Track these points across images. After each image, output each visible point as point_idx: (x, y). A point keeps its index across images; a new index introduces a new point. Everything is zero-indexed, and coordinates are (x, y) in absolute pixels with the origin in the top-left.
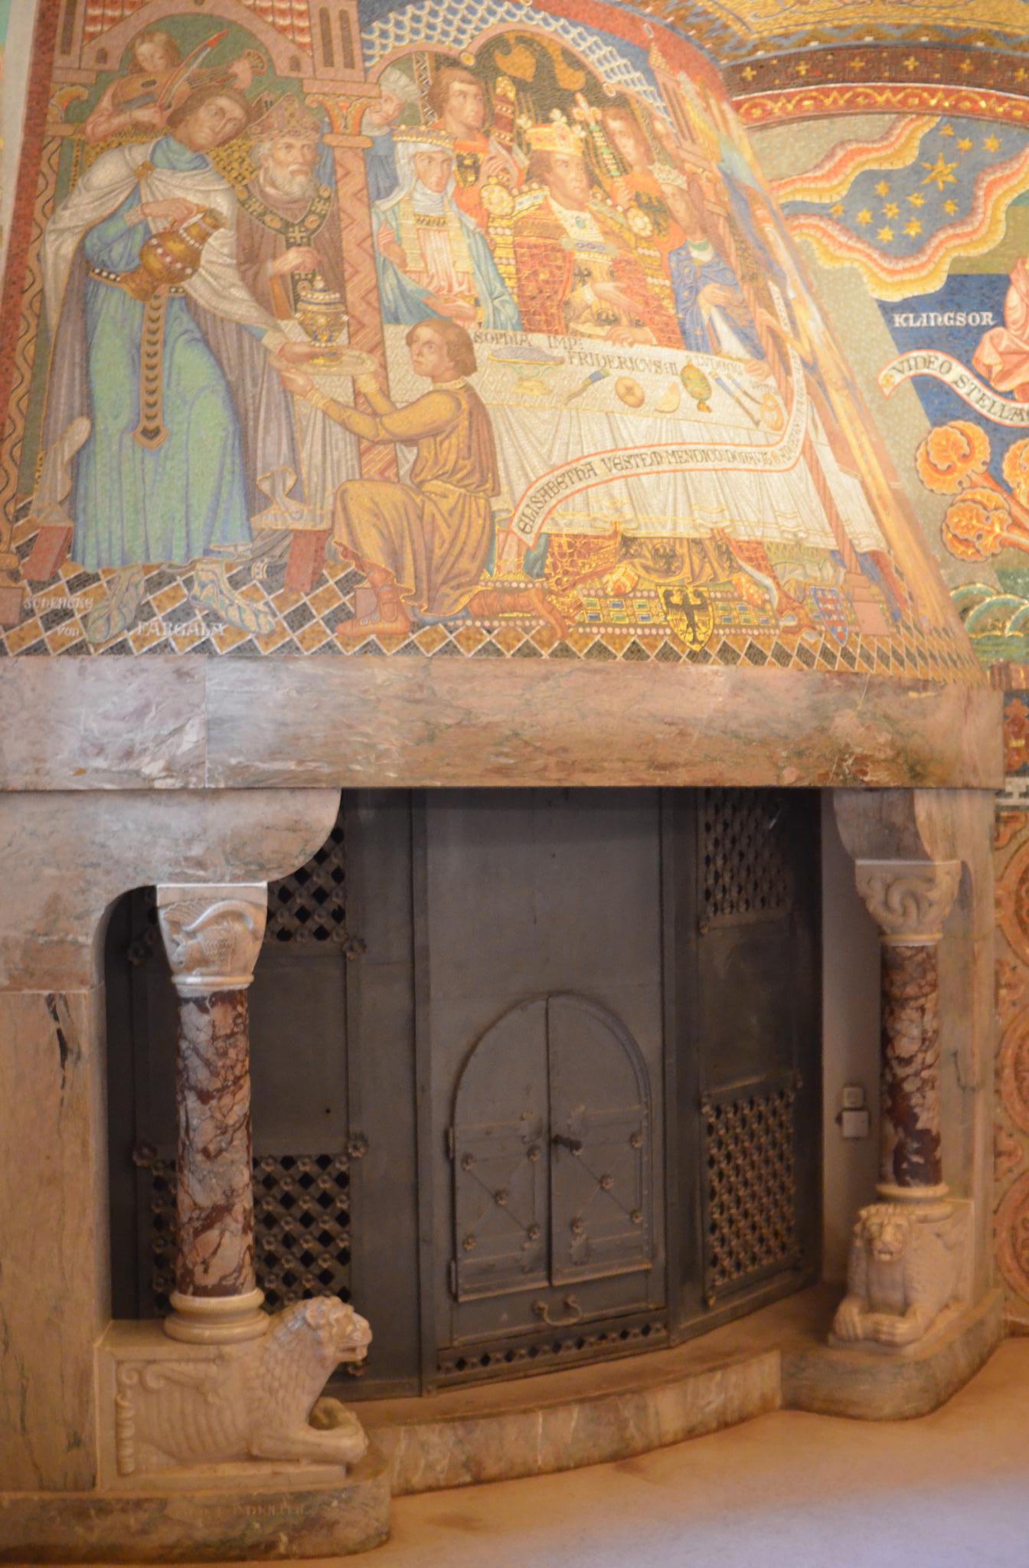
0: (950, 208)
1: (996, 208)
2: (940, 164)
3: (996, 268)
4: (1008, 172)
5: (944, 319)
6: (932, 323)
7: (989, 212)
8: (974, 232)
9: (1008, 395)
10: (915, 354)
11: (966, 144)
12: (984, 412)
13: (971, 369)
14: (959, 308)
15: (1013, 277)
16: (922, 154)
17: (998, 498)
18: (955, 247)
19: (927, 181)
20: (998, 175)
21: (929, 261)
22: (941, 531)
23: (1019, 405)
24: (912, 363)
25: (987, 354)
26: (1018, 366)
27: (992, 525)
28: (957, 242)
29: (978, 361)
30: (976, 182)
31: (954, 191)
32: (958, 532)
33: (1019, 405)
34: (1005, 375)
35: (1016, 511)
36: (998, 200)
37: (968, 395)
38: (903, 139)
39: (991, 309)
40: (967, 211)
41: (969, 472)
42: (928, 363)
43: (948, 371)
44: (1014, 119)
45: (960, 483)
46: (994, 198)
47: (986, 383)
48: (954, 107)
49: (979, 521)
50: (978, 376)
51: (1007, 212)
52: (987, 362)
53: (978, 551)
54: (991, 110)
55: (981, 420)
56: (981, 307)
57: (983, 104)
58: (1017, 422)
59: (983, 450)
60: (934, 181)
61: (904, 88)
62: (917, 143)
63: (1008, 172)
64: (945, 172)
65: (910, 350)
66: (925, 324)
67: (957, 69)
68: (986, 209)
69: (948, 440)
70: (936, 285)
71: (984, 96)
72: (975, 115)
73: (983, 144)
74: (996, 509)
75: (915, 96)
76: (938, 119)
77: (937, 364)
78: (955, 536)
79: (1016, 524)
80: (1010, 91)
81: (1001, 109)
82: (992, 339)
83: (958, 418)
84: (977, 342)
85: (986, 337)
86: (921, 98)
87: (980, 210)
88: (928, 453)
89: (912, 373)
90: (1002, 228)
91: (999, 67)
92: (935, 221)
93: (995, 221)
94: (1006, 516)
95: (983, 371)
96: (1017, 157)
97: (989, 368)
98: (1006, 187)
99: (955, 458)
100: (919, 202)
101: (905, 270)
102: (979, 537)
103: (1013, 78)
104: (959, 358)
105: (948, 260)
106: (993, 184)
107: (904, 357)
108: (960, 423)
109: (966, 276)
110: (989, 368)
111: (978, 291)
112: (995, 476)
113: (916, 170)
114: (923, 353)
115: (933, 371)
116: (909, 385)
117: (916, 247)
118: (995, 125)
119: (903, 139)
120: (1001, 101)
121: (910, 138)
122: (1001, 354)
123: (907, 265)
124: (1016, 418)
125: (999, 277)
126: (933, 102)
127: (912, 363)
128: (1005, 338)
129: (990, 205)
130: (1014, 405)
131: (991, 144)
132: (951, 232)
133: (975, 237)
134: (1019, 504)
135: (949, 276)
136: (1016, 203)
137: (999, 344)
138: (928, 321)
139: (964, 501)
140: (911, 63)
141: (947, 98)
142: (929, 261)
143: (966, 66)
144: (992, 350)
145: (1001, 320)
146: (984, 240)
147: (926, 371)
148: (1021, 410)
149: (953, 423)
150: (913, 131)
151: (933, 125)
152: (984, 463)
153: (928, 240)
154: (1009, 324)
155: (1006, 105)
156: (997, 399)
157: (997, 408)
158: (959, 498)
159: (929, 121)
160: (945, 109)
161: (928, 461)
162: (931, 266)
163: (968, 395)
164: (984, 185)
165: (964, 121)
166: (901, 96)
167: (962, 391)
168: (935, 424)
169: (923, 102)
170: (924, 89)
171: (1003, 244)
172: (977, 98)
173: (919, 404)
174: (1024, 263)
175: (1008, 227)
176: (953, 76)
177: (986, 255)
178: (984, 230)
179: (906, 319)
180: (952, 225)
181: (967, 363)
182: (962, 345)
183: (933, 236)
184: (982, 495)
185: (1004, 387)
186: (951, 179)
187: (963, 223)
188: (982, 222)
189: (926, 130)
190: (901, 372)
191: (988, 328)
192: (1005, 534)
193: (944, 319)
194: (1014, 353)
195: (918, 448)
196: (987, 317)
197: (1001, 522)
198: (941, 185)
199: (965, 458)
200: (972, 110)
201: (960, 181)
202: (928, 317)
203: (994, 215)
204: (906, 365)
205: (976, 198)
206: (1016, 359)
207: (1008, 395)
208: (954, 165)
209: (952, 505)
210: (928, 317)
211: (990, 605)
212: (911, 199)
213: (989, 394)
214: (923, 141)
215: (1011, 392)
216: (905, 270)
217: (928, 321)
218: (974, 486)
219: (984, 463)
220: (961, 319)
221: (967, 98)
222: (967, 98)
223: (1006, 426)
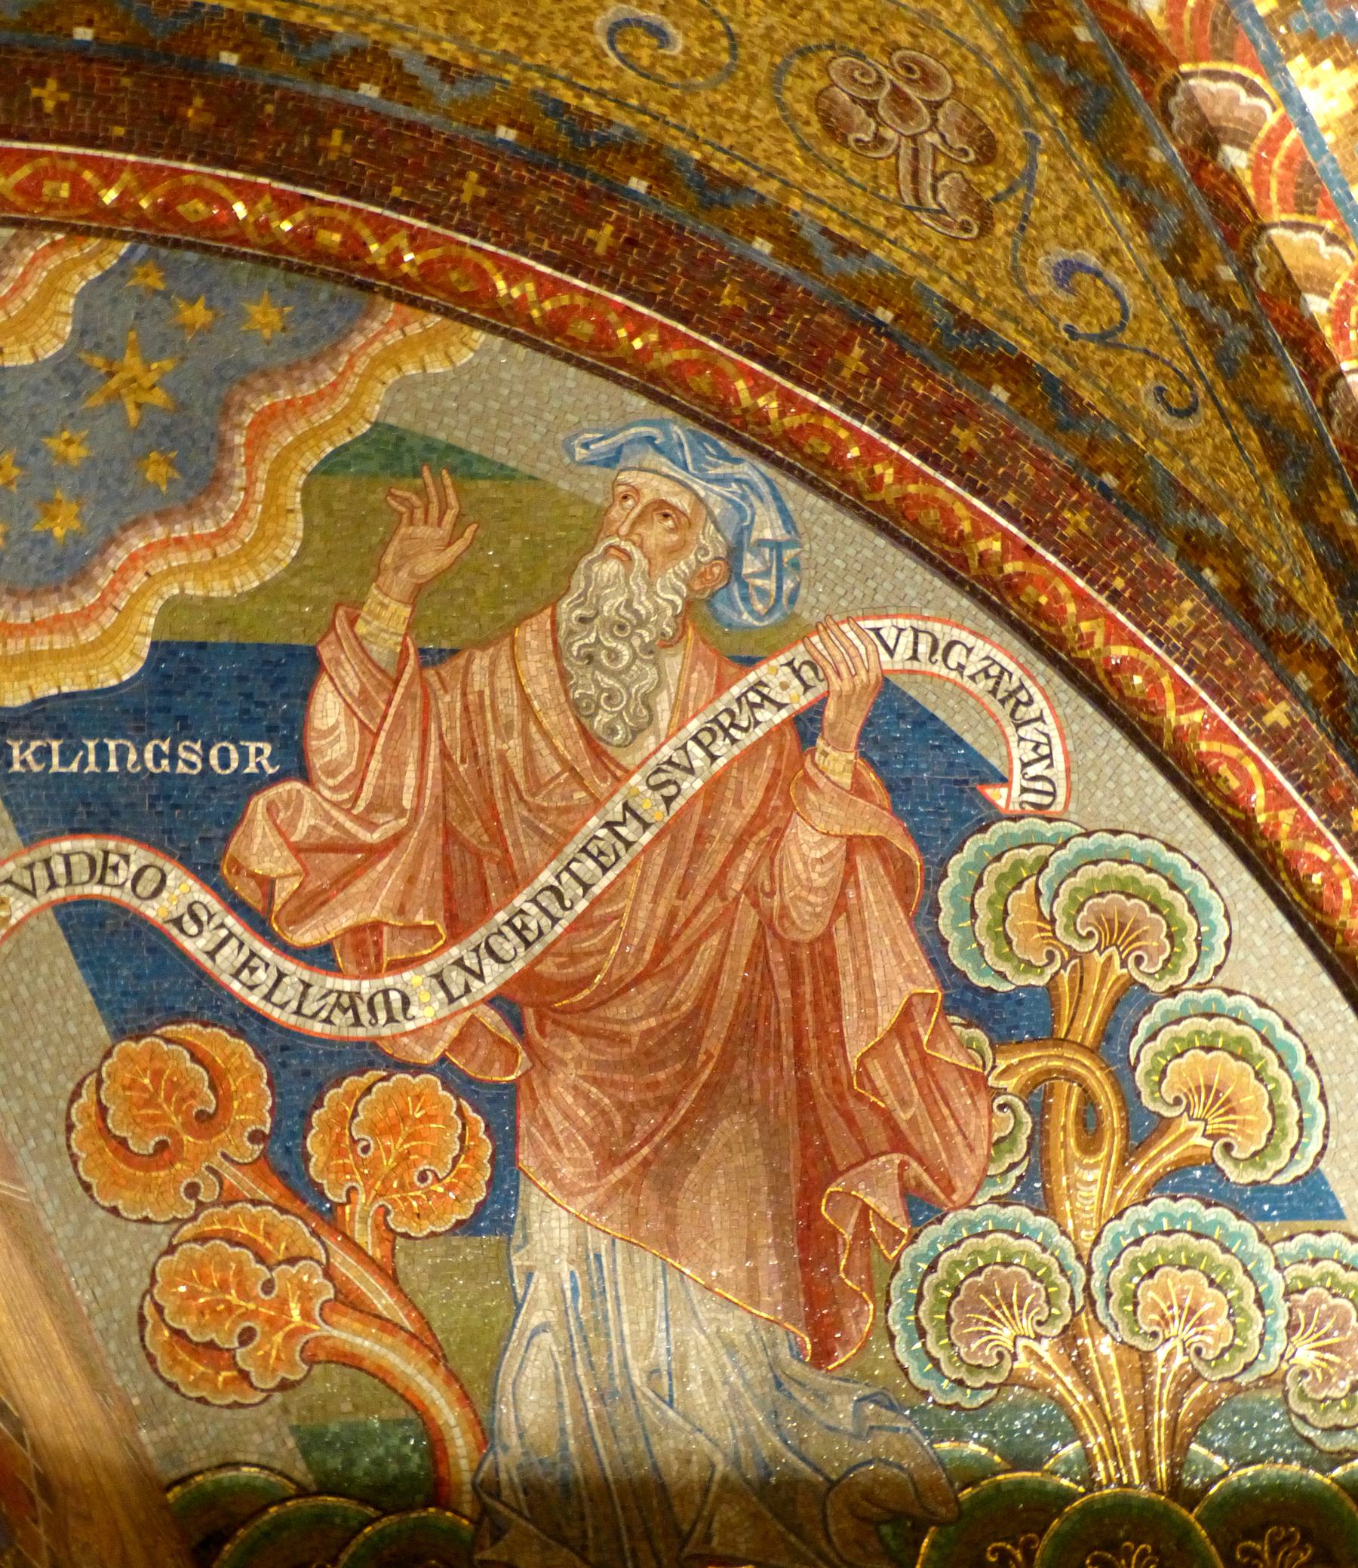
0: (156, 471)
1: (277, 477)
2: (132, 362)
3: (277, 630)
4: (307, 389)
5: (146, 757)
6: (113, 767)
7: (261, 488)
8: (223, 534)
9: (321, 957)
10: (66, 845)
11: (198, 314)
12: (254, 999)
13: (219, 889)
14: (183, 727)
15: (326, 653)
16: (82, 332)
17: (295, 1229)
18: (171, 571)
19: (97, 401)
20: (283, 395)
21: (103, 603)
22: (142, 1320)
23: (348, 985)
24: (59, 868)
25: (261, 848)
26: (343, 881)
27: (283, 1304)
28: (178, 558)
29: (238, 868)
30: (225, 409)
31: (166, 431)
32: (186, 1324)
33: (348, 985)
34: (309, 904)
35: (346, 1265)
36: (281, 461)
37: (212, 954)
38: (30, 293)
39: (269, 733)
40: (203, 483)
41: (217, 1161)
42: (100, 868)
43: (156, 893)
44: (321, 254)
45: (193, 1190)
46: (272, 453)
47: (259, 922)
48: (166, 210)
49: (244, 1294)
50: (236, 905)
51: (306, 490)
52: (262, 866)
53: (244, 1375)
54: (264, 227)
55: (246, 1022)
56: (245, 727)
57: (240, 209)
58: (342, 1026)
59: (254, 1104)
60: (114, 400)
61: (32, 155)
62: (69, 304)
63: (307, 389)
64: (146, 380)
65: (55, 836)
66: (92, 767)
67: (172, 117)
68: (252, 482)
69: (157, 1076)
70: (124, 665)
71: (241, 190)
72: (220, 243)
73: (242, 315)
74: (292, 1261)
75: (58, 175)
76: (124, 248)
77: (125, 874)
78: (178, 1333)
79: (348, 1301)
80: (308, 185)
81: (286, 226)
82: (271, 809)
83: (183, 1017)
84: (233, 818)
85: (259, 803)
86: (75, 180)
87: (238, 482)
88: (103, 1110)
89: (59, 894)
90: (296, 525)
91: (278, 120)
92: (120, 504)
93: (274, 509)
94: (318, 1280)
95: (249, 892)
96: (335, 351)
97: (267, 884)
98: (302, 427)
99: (176, 1121)
100: (76, 453)
101: (36, 625)
102: (247, 1336)
103: (315, 152)
104: (185, 860)
105: (155, 605)
106: (269, 417)
107: (37, 854)
108: (189, 1030)
109: (202, 646)
110: (267, 884)
111: (234, 686)
112: (284, 1163)
113: (66, 371)
114: (89, 844)
115: (116, 890)
116: (49, 927)
117: (70, 568)
118: (273, 272)
119: (30, 293)
120: (287, 205)
121: (51, 290)
122: (297, 850)
123: (44, 613)
124: (337, 1017)
125: (290, 651)
126: (110, 196)
127: (59, 868)
128: (309, 810)
129: (262, 472)
130: (332, 982)
131: (264, 317)
132: (159, 532)
133: (223, 550)
134: (358, 1250)
135: (154, 645)
136: (330, 466)
137: (293, 823)
138: (102, 762)
139: (202, 1239)
140: (49, 94)
141: (145, 187)
142: (103, 603)
143: (195, 112)
144: (274, 839)
145: (296, 764)
146: (247, 555)
147: (97, 890)
148: (354, 996)
149: (170, 1030)
150: (61, 272)
151: (110, 261)
152: (255, 1137)
153: (102, 551)
154: (318, 773)
155: (299, 216)
156: (288, 966)
157: (289, 991)
158: (188, 1230)
159: (101, 251)
160: (141, 220)
161: (105, 1132)
162: (109, 618)
163: (212, 954)
164: (247, 419)
165: (192, 256)
166: (23, 172)
167: (195, 946)
168: (120, 1033)
169: (83, 195)
170: (84, 161)
171: (297, 567)
172: (225, 193)
173: (77, 975)
174: (352, 622)
175: (308, 525)
176: (160, 132)
177: (252, 595)
178: (247, 531)
179: (44, 754)
180: (164, 516)
181: (207, 872)
182: (194, 825)
183: (112, 540)
184: (253, 1225)
185: (306, 936)
186: (158, 398)
187: (192, 509)
188: (242, 513)
189: (94, 273)
190: (33, 893)
191: (260, 782)
192: (319, 1329)
193: (146, 757)
194: (332, 847)
195: (76, 1095)
196: (260, 755)
197: (306, 1295)
198: (133, 414)
199: (205, 1123)
200: (211, 223)
201: (182, 406)
202: (102, 749)
203: (272, 496)
204: (40, 872)
205: (225, 448)
206: (336, 863)
207: (321, 957)
208: (168, 365)
209: (171, 1249)
210: (102, 749)
211: (279, 1524)
212: (55, 444)
213: (267, 953)
214: (85, 299)
215: (326, 948)
216: (36, 625)
217: (102, 762)
218: (227, 1198)
219: (255, 1137)
220: (190, 757)
221: (198, 192)
222: (198, 192)
223: (311, 1038)
